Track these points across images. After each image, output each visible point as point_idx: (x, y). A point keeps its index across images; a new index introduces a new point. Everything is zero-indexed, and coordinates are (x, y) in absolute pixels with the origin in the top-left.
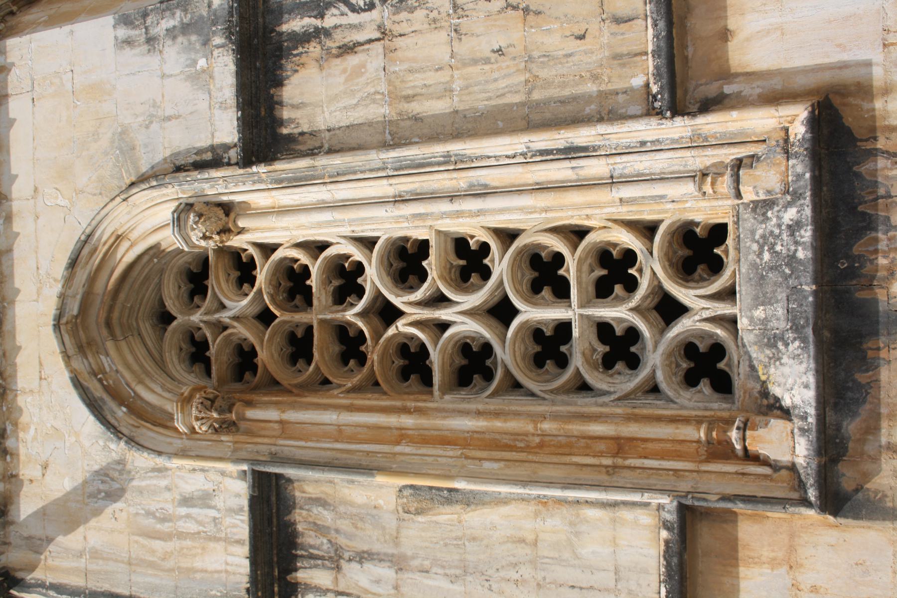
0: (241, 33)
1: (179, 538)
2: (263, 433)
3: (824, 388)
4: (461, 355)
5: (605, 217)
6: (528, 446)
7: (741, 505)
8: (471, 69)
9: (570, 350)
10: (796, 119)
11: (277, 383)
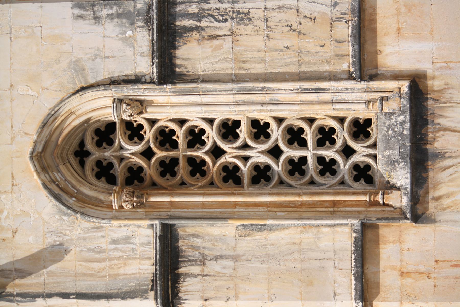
1: (109, 260)
10: (405, 86)
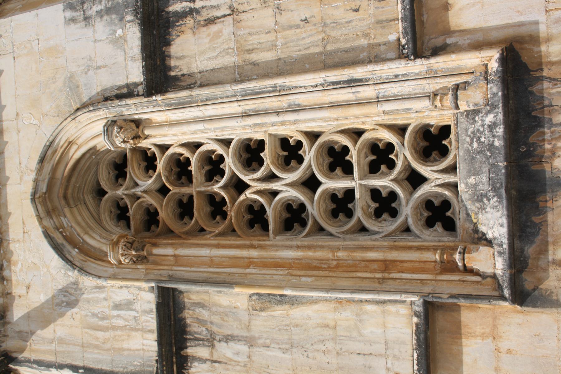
0: (143, 13)
1: (113, 330)
2: (164, 263)
3: (513, 226)
4: (286, 211)
5: (374, 122)
6: (329, 267)
7: (462, 301)
8: (288, 32)
9: (354, 206)
10: (492, 58)
11: (171, 231)
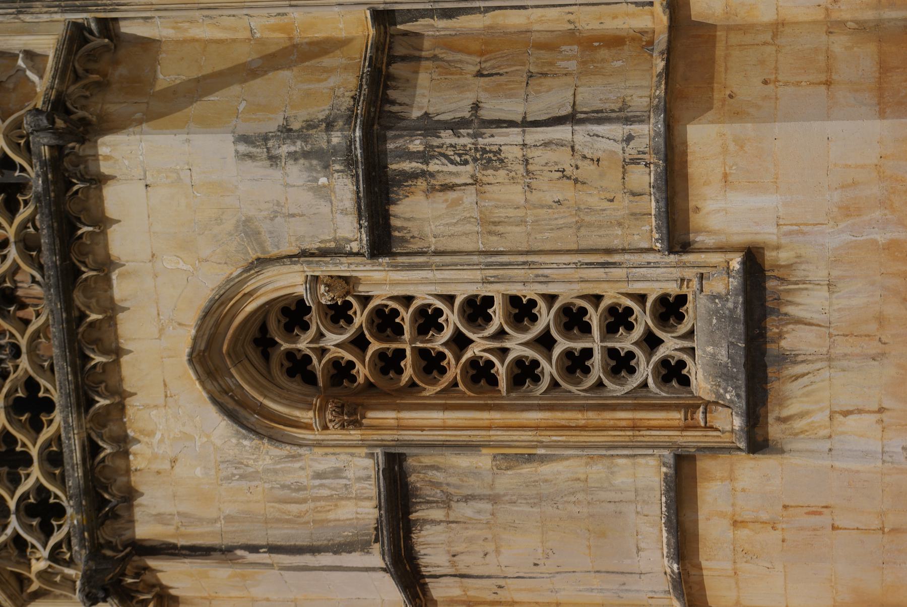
1: (313, 501)
